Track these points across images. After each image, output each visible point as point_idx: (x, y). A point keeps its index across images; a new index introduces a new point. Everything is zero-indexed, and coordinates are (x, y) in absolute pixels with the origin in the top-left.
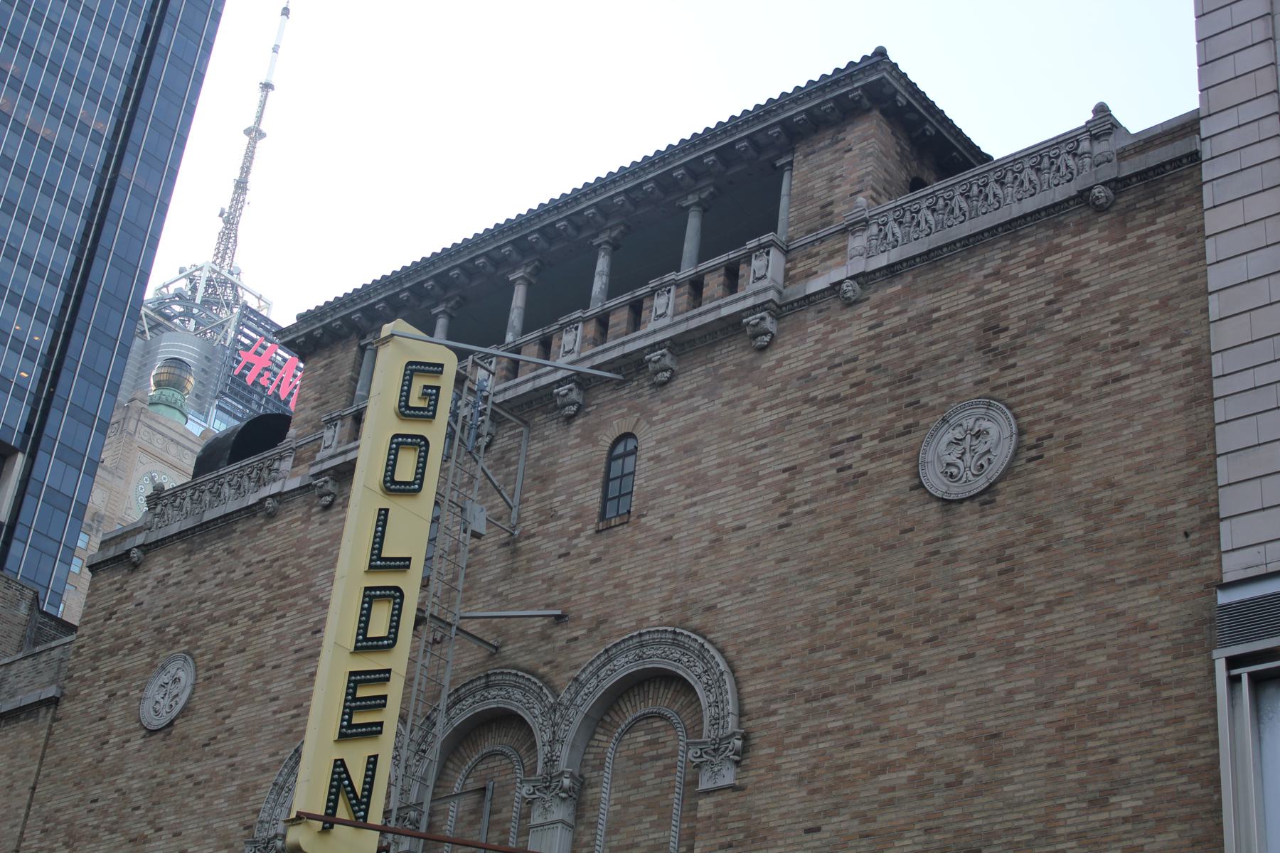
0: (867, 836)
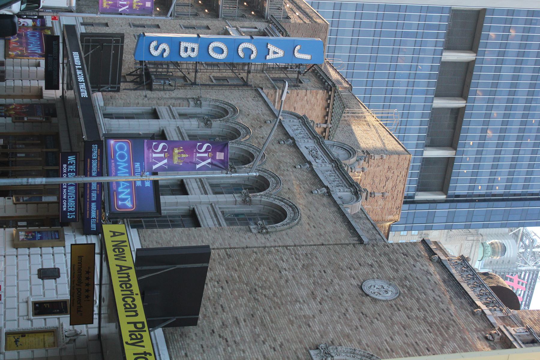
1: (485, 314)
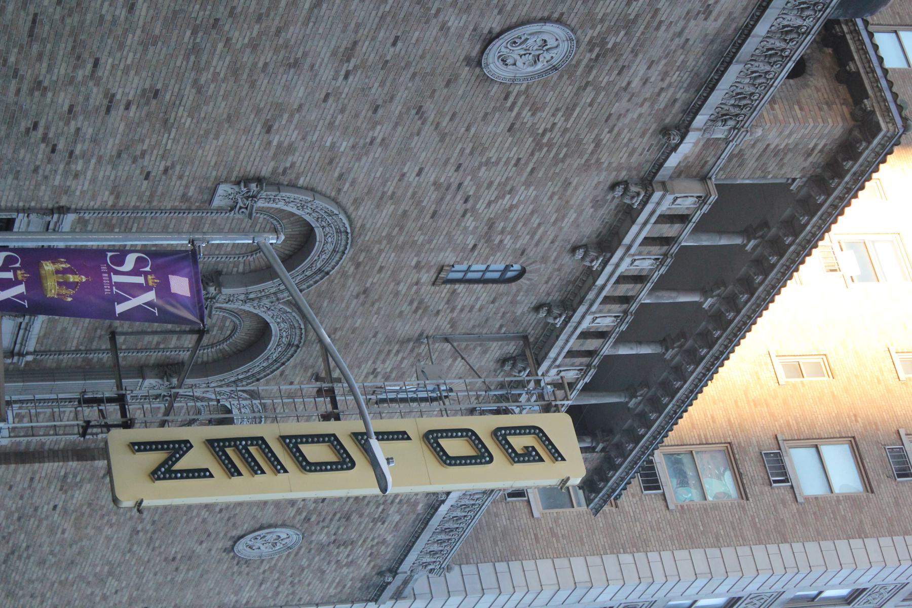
0: (38, 526)
1: (675, 148)
